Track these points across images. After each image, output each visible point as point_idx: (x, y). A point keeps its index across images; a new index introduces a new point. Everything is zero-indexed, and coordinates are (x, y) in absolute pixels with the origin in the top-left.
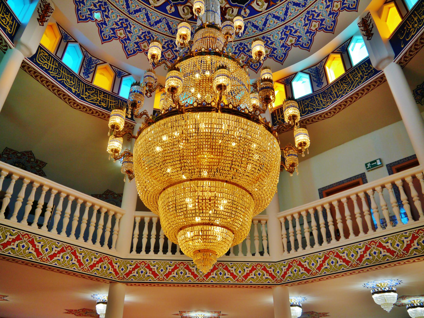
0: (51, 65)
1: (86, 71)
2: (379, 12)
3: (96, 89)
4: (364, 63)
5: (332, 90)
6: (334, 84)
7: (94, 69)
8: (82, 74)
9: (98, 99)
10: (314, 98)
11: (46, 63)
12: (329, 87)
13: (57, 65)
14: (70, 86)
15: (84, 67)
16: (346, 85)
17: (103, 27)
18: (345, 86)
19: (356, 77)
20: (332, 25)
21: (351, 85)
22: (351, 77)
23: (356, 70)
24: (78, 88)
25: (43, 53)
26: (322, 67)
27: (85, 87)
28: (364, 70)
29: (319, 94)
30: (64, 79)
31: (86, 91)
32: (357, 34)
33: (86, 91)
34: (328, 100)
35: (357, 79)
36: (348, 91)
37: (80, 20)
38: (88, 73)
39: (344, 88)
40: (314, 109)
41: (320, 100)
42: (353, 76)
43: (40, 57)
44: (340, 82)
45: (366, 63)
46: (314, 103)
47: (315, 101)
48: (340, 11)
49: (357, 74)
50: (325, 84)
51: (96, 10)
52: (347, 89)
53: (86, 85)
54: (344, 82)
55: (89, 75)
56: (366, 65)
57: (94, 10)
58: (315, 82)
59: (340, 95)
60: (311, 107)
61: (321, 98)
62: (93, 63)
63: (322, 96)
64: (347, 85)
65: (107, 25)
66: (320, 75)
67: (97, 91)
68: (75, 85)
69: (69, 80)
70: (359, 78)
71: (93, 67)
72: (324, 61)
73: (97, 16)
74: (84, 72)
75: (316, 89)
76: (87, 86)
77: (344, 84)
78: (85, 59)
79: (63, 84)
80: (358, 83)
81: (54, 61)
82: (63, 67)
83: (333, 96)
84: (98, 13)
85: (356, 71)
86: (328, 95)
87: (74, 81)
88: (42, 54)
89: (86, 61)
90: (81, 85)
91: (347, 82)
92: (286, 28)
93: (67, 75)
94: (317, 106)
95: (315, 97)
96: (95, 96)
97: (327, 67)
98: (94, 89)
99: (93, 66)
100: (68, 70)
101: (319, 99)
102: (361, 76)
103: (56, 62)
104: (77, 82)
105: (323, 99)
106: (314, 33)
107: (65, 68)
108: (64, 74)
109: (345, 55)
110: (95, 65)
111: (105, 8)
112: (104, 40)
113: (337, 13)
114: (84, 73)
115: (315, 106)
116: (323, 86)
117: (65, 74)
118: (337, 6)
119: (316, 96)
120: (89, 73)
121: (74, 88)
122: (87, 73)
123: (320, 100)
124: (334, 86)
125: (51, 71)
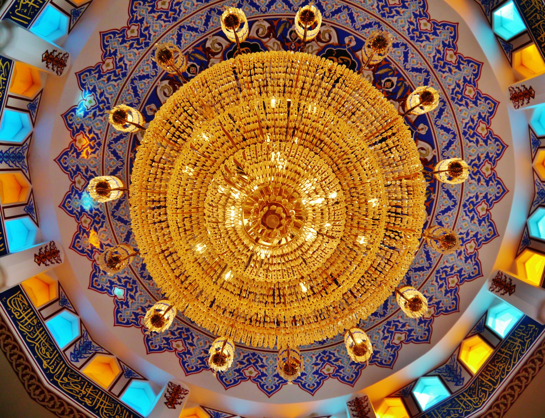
0: (26, 318)
1: (76, 353)
2: (513, 268)
3: (82, 378)
4: (519, 327)
5: (483, 382)
6: (483, 371)
7: (90, 355)
8: (68, 353)
9: (81, 392)
10: (455, 400)
11: (19, 311)
12: (476, 379)
13: (36, 323)
14: (43, 357)
15: (75, 346)
16: (502, 363)
17: (122, 307)
18: (501, 365)
19: (514, 348)
20: (453, 303)
21: (510, 359)
22: (506, 351)
23: (509, 340)
24: (53, 366)
25: (22, 299)
26: (456, 361)
27: (67, 370)
28: (522, 335)
29: (462, 394)
30: (37, 344)
31: (65, 375)
32: (494, 303)
33: (65, 375)
34: (481, 394)
35: (517, 348)
36: (508, 369)
37: (92, 286)
38: (79, 356)
39: (501, 369)
40: (462, 414)
41: (468, 400)
42: (509, 348)
43: (14, 301)
44: (492, 365)
45: (521, 326)
46: (459, 407)
47: (458, 403)
48: (458, 285)
49: (513, 344)
50: (467, 378)
51: (119, 285)
52: (506, 368)
53: (68, 368)
54: (497, 362)
55: (79, 359)
56: (522, 328)
57: (116, 284)
58: (451, 382)
59: (497, 380)
60: (455, 413)
61: (467, 398)
62: (92, 349)
63: (469, 395)
64: (504, 362)
65: (128, 307)
66: (455, 372)
67: (85, 383)
68: (51, 360)
69: (43, 349)
70: (519, 346)
71: (90, 353)
72: (456, 353)
73: (119, 292)
74: (73, 352)
75: (455, 389)
76: (69, 370)
77: (498, 364)
78: (82, 339)
79: (32, 349)
80: (520, 353)
81: (32, 316)
82: (44, 329)
83: (486, 388)
84: (120, 289)
85: (511, 341)
86: (479, 389)
87: (51, 355)
88: (20, 299)
89: (82, 342)
90: (61, 366)
91: (502, 360)
92: (389, 323)
93: (44, 341)
94: (464, 409)
95: (456, 399)
96: (78, 387)
97: (462, 358)
98: (80, 378)
99: (90, 352)
100: (49, 337)
101: (465, 399)
102: (520, 343)
103: (35, 318)
104: (57, 358)
105: (472, 397)
106: (431, 321)
107: (46, 332)
108: (40, 339)
109: (485, 333)
110: (94, 352)
111: (132, 286)
112: (118, 322)
113: (456, 288)
114: (71, 354)
115: (461, 410)
116: (465, 383)
117: (42, 339)
118: (453, 282)
119: (458, 397)
120: (81, 358)
121: (48, 363)
122: (77, 355)
123: (468, 400)
124: (483, 373)
125: (22, 324)
